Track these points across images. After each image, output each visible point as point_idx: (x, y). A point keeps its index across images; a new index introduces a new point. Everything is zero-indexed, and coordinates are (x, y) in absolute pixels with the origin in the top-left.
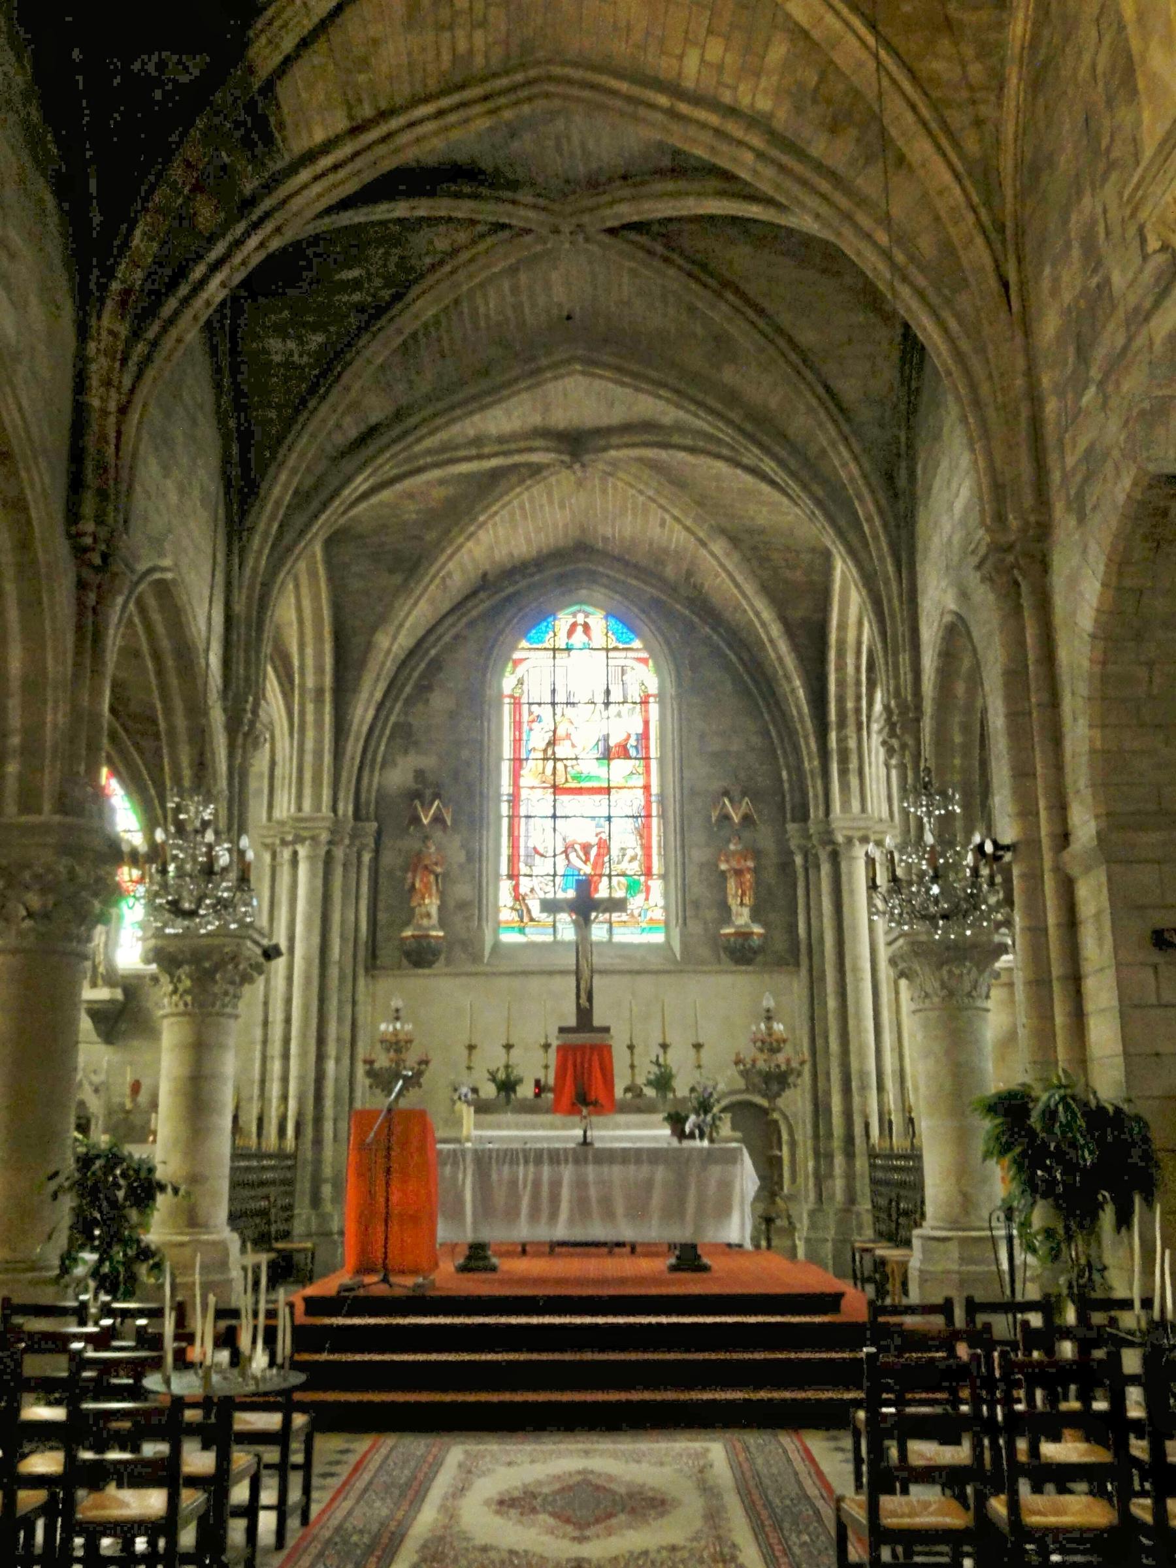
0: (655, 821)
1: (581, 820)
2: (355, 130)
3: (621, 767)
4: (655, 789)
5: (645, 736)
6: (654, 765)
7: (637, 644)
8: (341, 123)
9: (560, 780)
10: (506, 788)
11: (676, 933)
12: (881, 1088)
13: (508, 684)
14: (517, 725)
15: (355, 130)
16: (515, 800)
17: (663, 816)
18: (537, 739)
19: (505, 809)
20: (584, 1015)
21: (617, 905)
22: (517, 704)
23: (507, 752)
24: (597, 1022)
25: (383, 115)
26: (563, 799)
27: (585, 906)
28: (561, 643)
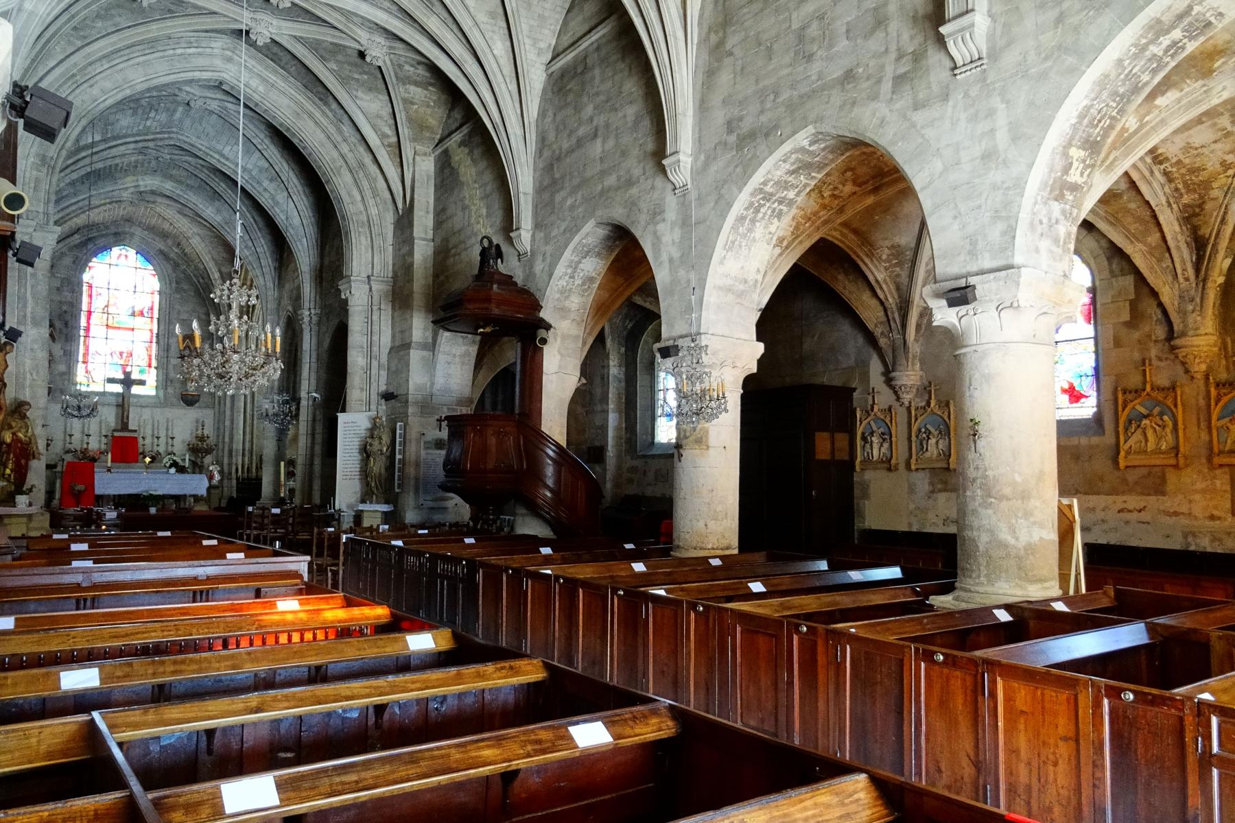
0: (154, 345)
1: (120, 341)
2: (104, 141)
3: (139, 322)
4: (155, 331)
5: (152, 309)
6: (155, 321)
7: (151, 267)
8: (98, 138)
9: (110, 323)
10: (83, 323)
11: (161, 393)
12: (243, 455)
13: (86, 277)
14: (90, 296)
15: (104, 141)
16: (87, 329)
17: (158, 342)
18: (98, 304)
19: (82, 333)
20: (124, 426)
21: (142, 383)
22: (90, 287)
23: (85, 307)
24: (131, 427)
25: (114, 138)
26: (110, 331)
27: (128, 382)
28: (114, 261)
